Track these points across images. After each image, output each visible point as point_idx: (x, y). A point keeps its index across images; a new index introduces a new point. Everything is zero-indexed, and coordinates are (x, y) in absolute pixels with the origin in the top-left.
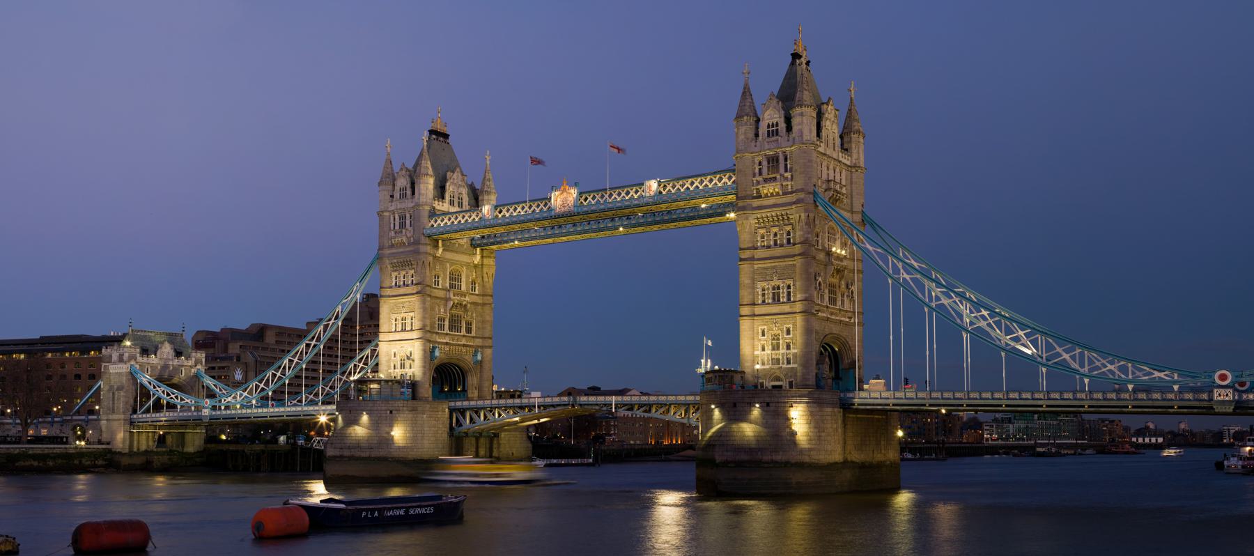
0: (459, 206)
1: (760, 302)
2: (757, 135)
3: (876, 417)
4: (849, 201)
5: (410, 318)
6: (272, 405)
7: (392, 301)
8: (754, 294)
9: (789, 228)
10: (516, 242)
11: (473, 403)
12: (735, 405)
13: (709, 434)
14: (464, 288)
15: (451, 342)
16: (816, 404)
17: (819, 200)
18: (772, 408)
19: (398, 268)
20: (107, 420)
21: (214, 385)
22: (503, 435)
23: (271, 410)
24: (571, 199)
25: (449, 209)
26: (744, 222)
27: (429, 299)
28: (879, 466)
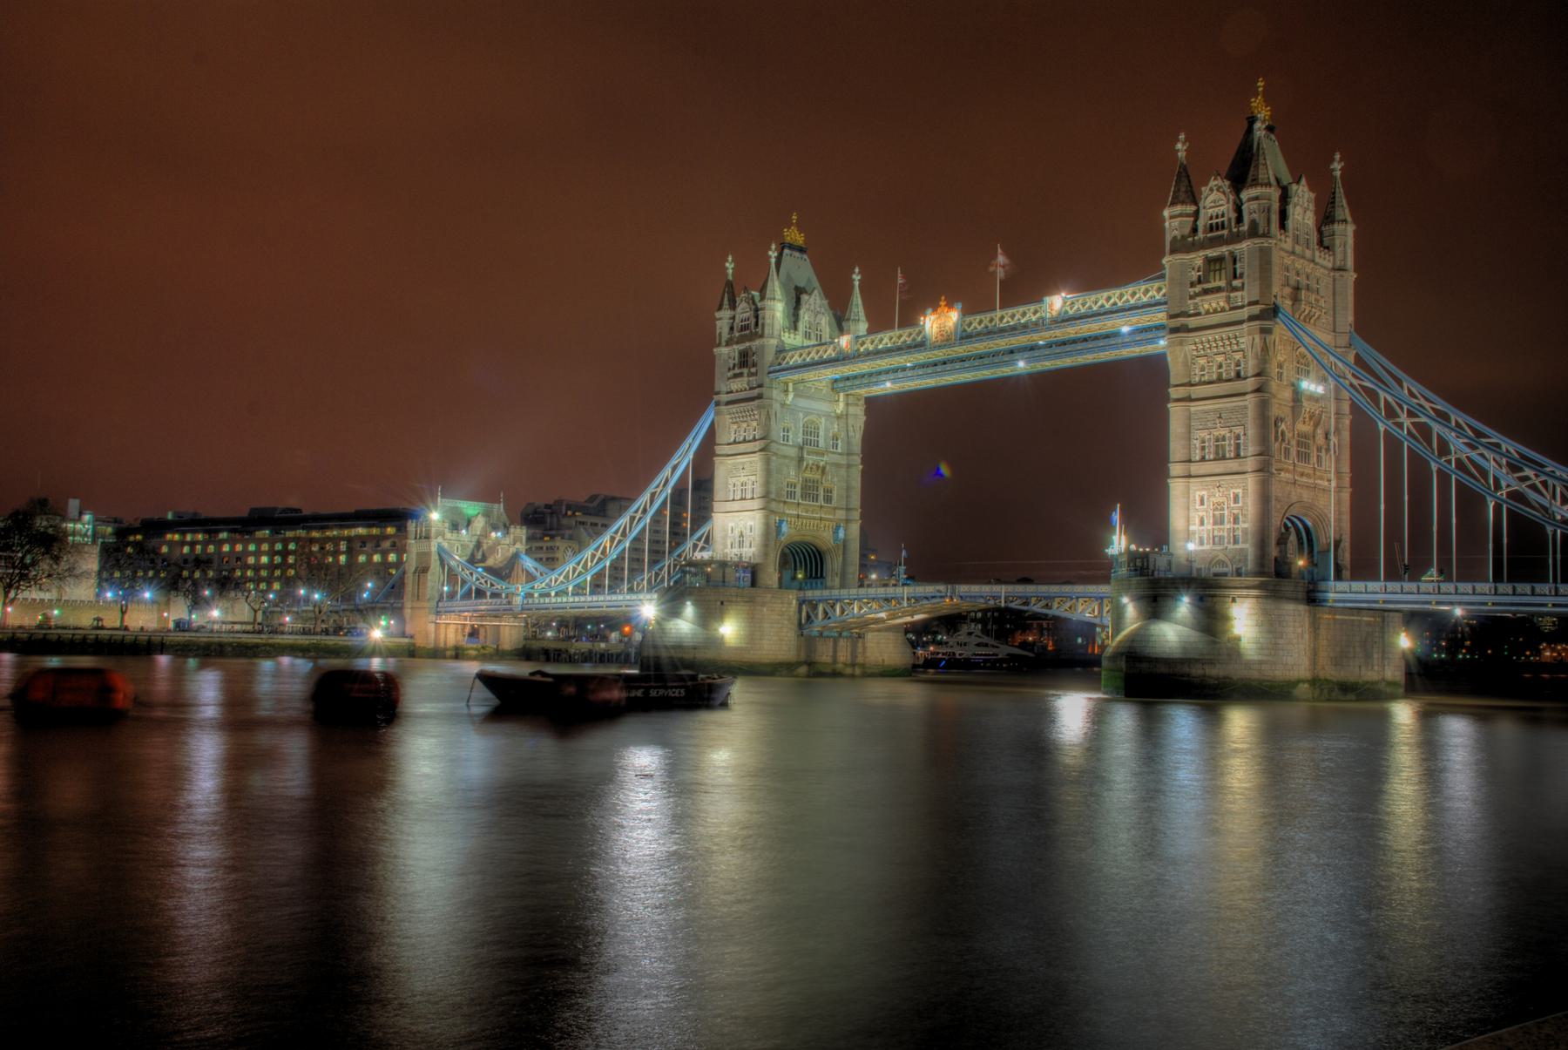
0: (817, 339)
1: (1198, 458)
3: (1365, 619)
4: (1331, 319)
5: (750, 483)
7: (730, 461)
8: (1189, 447)
9: (1238, 356)
13: (1119, 638)
14: (821, 443)
15: (804, 514)
19: (738, 419)
20: (412, 608)
22: (869, 636)
23: (589, 599)
26: (1178, 348)
27: (774, 458)
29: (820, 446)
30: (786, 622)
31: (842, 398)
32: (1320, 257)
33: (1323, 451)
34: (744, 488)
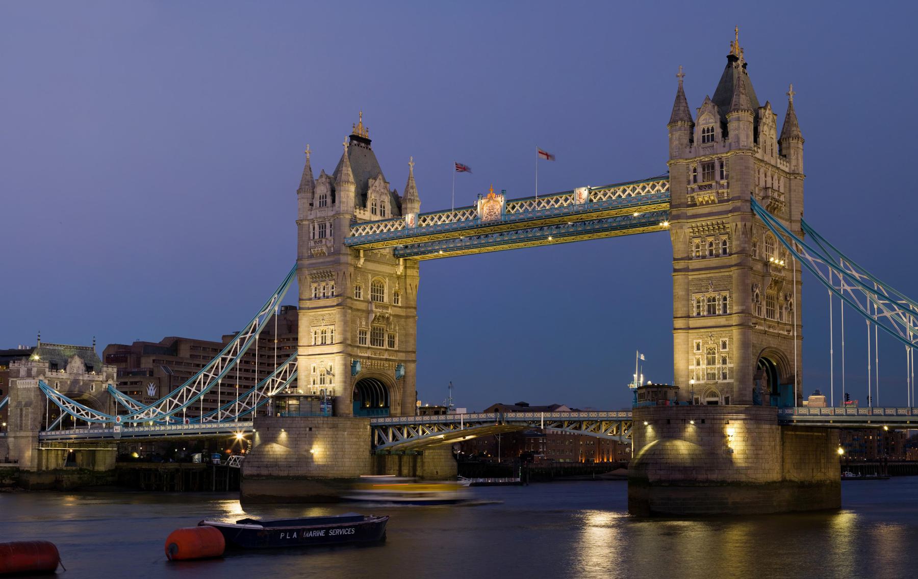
0: (381, 215)
1: (695, 314)
2: (691, 141)
5: (330, 331)
6: (187, 422)
7: (312, 313)
8: (688, 306)
9: (725, 237)
10: (441, 252)
11: (395, 420)
12: (669, 422)
13: (642, 452)
14: (386, 299)
15: (373, 356)
16: (753, 420)
17: (756, 207)
18: (707, 425)
21: (126, 401)
22: (427, 453)
23: (186, 427)
24: (498, 207)
25: (370, 217)
26: (679, 231)
28: (820, 485)
29: (385, 301)
30: (362, 444)
31: (401, 263)
32: (781, 163)
33: (784, 309)
34: (324, 335)
